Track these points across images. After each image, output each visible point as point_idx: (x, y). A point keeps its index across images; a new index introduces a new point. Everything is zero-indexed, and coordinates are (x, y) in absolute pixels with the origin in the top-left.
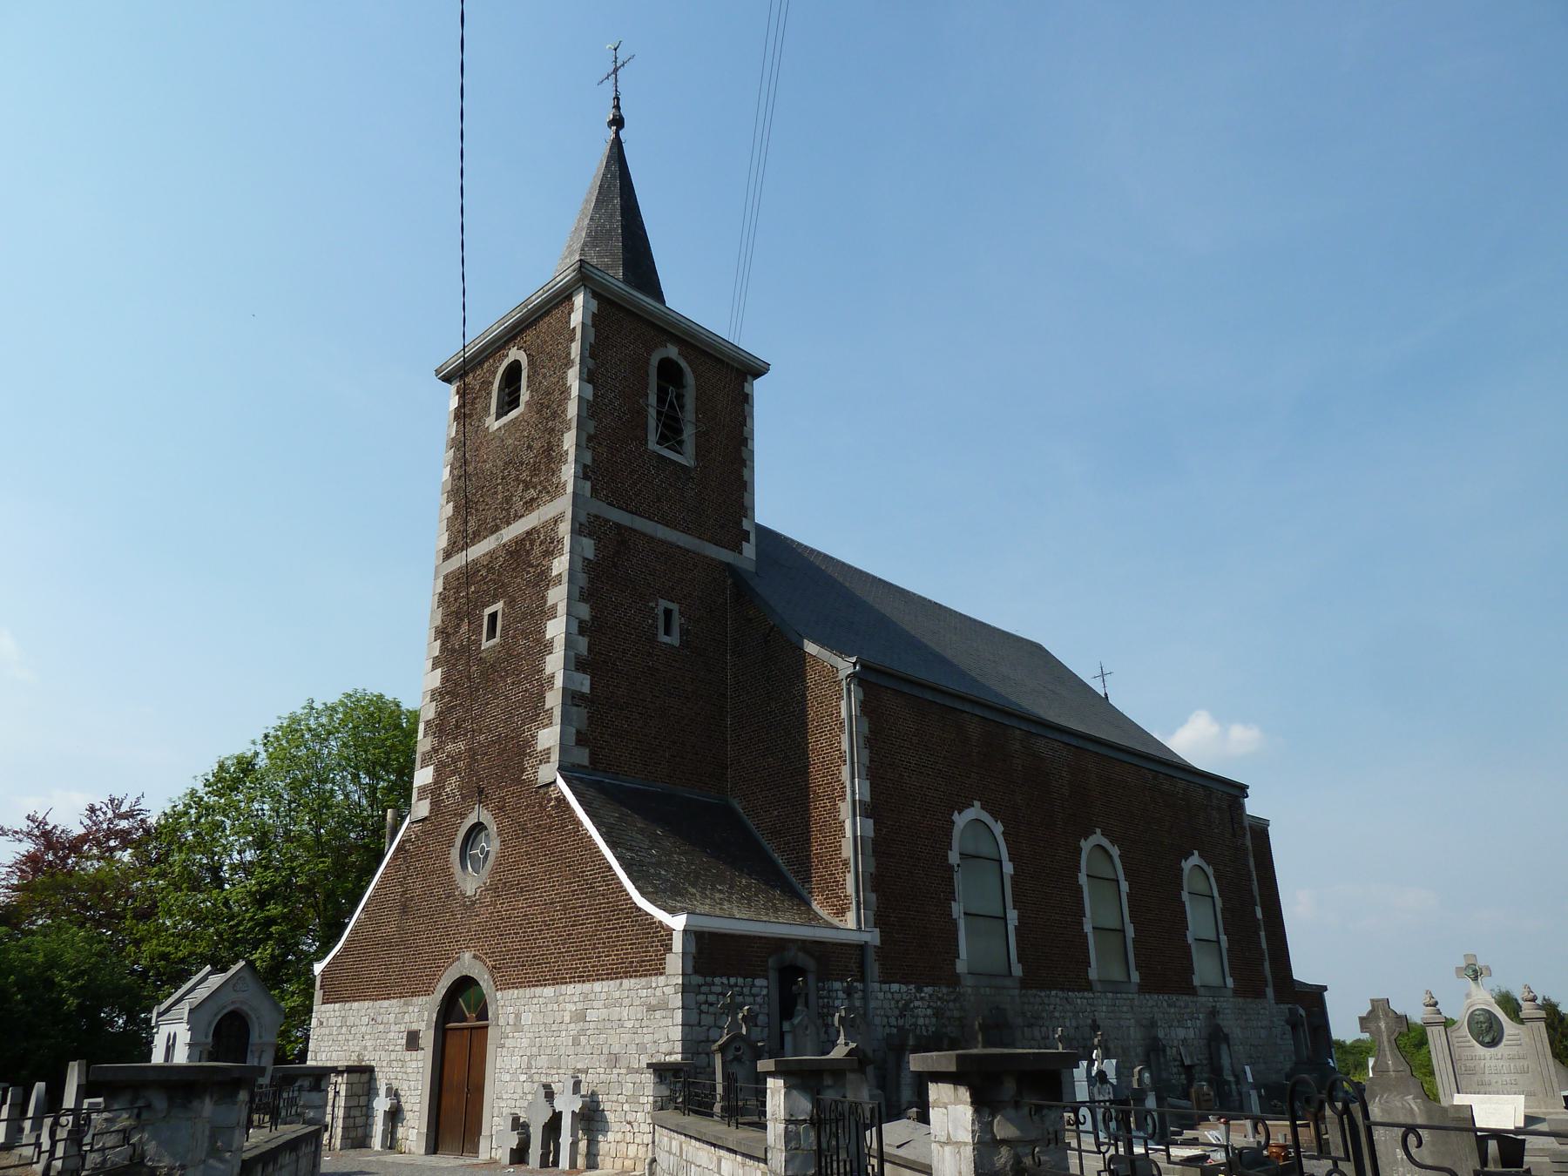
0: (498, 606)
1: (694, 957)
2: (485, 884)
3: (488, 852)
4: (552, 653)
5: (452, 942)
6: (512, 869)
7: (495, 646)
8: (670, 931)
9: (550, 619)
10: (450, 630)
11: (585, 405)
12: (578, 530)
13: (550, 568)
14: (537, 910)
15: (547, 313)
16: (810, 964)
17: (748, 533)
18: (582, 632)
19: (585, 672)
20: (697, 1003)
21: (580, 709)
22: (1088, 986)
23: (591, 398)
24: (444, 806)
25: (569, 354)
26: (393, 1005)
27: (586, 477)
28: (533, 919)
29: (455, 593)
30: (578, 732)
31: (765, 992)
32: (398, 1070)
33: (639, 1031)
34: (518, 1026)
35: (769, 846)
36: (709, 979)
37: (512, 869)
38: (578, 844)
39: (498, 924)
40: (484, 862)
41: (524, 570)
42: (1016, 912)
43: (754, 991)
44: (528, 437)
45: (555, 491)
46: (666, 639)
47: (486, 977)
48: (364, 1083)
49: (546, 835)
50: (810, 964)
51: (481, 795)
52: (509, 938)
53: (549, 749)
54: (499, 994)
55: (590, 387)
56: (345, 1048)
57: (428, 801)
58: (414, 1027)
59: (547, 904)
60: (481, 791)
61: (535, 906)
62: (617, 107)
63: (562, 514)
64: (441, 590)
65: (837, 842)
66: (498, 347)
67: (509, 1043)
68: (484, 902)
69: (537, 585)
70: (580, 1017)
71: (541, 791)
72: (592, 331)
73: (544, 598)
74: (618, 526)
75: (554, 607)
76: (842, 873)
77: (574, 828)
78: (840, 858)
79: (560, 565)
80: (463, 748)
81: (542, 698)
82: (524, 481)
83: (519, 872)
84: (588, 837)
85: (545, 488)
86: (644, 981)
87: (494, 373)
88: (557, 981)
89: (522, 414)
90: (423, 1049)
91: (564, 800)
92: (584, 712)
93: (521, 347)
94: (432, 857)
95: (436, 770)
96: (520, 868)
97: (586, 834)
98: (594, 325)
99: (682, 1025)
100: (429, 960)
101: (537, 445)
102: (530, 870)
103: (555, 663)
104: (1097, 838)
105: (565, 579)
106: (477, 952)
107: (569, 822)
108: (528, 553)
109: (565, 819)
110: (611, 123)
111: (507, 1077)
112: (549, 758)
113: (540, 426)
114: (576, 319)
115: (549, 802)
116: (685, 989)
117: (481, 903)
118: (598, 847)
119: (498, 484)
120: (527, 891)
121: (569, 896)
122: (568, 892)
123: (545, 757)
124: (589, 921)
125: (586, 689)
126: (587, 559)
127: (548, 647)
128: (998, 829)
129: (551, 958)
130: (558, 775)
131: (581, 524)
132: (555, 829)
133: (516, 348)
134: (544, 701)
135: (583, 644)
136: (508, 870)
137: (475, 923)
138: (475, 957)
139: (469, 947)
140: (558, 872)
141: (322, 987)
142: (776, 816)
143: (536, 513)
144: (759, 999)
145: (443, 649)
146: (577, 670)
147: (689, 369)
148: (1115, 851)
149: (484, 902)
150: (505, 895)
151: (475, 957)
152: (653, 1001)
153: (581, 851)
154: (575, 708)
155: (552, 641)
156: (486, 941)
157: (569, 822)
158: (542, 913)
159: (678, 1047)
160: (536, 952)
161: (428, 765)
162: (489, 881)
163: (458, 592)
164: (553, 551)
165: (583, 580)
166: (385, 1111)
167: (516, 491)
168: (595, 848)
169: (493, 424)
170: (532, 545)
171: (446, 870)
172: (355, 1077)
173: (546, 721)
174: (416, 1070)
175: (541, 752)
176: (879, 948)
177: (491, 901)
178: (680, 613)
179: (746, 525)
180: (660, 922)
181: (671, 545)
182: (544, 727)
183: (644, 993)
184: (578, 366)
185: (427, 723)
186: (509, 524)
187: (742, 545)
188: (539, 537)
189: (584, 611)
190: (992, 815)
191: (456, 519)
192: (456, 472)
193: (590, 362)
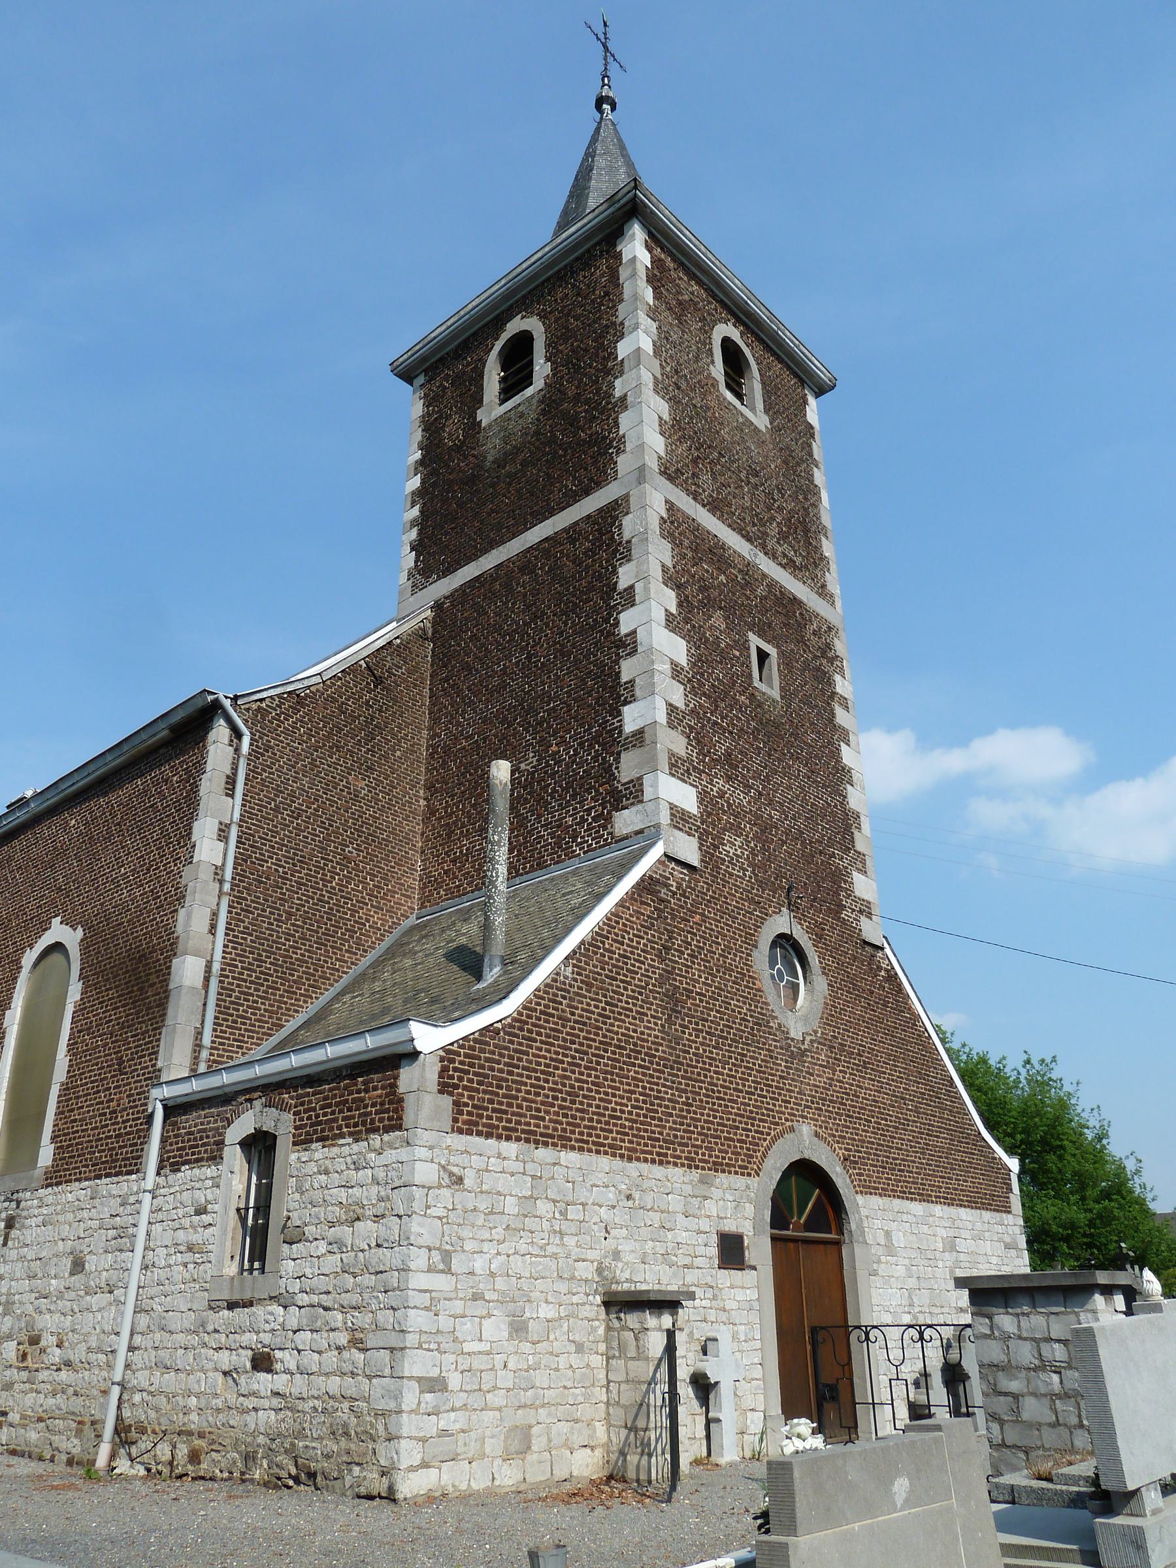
32: (705, 1303)
34: (890, 1250)
54: (859, 1198)
56: (550, 1249)
58: (730, 1227)
67: (882, 1269)
88: (924, 1198)
90: (754, 1268)
138: (817, 1135)
174: (747, 1306)
180: (1000, 1159)
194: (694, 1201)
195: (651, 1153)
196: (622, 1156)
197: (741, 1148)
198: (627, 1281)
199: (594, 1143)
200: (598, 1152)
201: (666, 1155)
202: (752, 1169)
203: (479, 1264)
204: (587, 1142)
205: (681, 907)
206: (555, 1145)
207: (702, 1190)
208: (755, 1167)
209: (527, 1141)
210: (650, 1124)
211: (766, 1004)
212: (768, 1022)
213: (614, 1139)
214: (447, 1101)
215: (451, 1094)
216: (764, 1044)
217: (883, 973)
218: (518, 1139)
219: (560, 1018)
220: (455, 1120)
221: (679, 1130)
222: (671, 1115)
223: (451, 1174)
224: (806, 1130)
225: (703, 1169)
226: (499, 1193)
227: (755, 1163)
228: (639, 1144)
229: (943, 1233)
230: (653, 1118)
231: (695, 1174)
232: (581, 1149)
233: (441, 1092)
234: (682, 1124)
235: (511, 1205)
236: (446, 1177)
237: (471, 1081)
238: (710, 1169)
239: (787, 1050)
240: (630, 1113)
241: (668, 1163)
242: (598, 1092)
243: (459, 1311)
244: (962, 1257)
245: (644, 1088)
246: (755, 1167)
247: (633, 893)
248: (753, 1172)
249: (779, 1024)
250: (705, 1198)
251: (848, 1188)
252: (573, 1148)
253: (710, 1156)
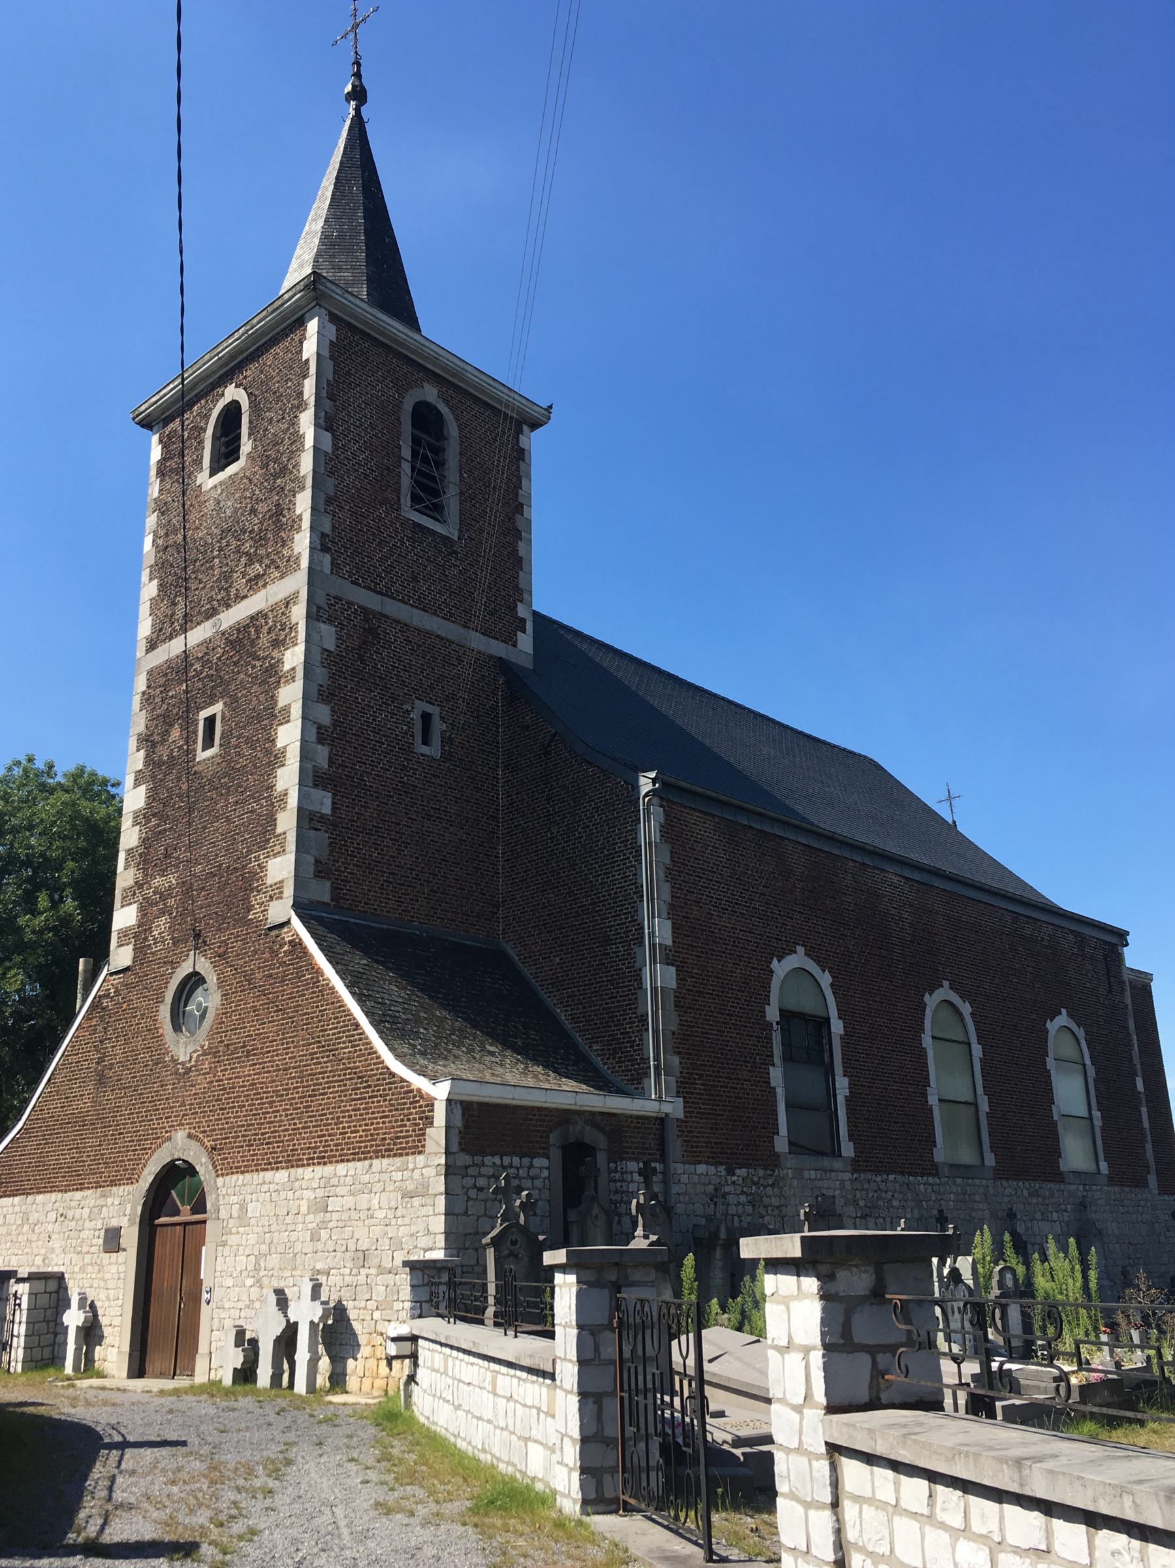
0: (217, 708)
1: (460, 1132)
2: (202, 1047)
3: (206, 1008)
4: (284, 765)
5: (162, 1118)
6: (237, 1029)
7: (213, 757)
8: (430, 1103)
9: (282, 724)
10: (156, 738)
11: (323, 457)
12: (314, 615)
13: (280, 661)
14: (267, 1078)
16: (601, 1141)
17: (524, 621)
18: (320, 741)
19: (325, 789)
20: (463, 1187)
21: (318, 833)
22: (933, 1169)
23: (329, 450)
24: (151, 953)
25: (301, 393)
26: (89, 1197)
27: (325, 549)
28: (262, 1088)
29: (161, 692)
30: (317, 862)
31: (545, 1173)
33: (393, 1222)
35: (549, 1000)
36: (478, 1159)
37: (237, 1029)
38: (318, 997)
39: (218, 1095)
40: (203, 1016)
41: (248, 663)
42: (846, 1080)
43: (533, 1172)
44: (251, 498)
45: (287, 566)
46: (424, 750)
47: (204, 1160)
48: (50, 1293)
49: (278, 987)
50: (601, 1141)
51: (198, 939)
52: (232, 1113)
53: (281, 882)
54: (220, 1181)
55: (328, 436)
56: (26, 1250)
57: (131, 947)
58: (114, 1223)
59: (280, 1070)
60: (197, 936)
61: (265, 1073)
62: (358, 75)
63: (296, 594)
64: (144, 688)
65: (632, 994)
66: (211, 384)
68: (202, 1069)
69: (264, 682)
71: (273, 933)
72: (329, 365)
73: (273, 699)
74: (365, 610)
75: (287, 709)
76: (638, 1031)
77: (312, 978)
78: (635, 1013)
79: (294, 657)
80: (174, 882)
81: (273, 821)
82: (247, 554)
83: (244, 1032)
84: (330, 989)
85: (273, 561)
86: (398, 1161)
87: (207, 417)
88: (293, 1163)
89: (242, 469)
90: (124, 1250)
91: (301, 944)
92: (324, 836)
93: (241, 384)
94: (136, 1016)
95: (141, 909)
96: (246, 1027)
97: (328, 984)
98: (331, 357)
99: (446, 1214)
100: (133, 1141)
101: (262, 508)
102: (259, 1030)
103: (288, 778)
104: (945, 992)
105: (300, 674)
107: (307, 970)
108: (253, 643)
109: (301, 967)
110: (349, 97)
111: (229, 1282)
112: (282, 893)
113: (266, 484)
114: (309, 348)
115: (281, 946)
116: (450, 1171)
117: (197, 1070)
118: (343, 1001)
119: (214, 558)
120: (254, 1055)
121: (307, 1060)
122: (305, 1055)
123: (276, 892)
124: (331, 1090)
125: (327, 809)
126: (327, 650)
127: (276, 759)
128: (825, 979)
129: (285, 1136)
130: (293, 913)
131: (319, 608)
132: (289, 980)
133: (234, 385)
134: (275, 825)
135: (322, 754)
136: (231, 1030)
137: (190, 1095)
138: (190, 1136)
139: (183, 1125)
140: (293, 1032)
142: (558, 964)
143: (263, 593)
144: (538, 1183)
145: (148, 761)
146: (316, 786)
147: (451, 417)
148: (966, 1009)
149: (202, 1069)
150: (227, 1060)
151: (190, 1136)
152: (410, 1187)
153: (322, 1006)
154: (313, 833)
155: (284, 751)
156: (204, 1117)
157: (307, 970)
158: (274, 1081)
159: (441, 1241)
160: (266, 1128)
161: (130, 904)
162: (207, 1043)
163: (166, 691)
164: (285, 639)
165: (321, 676)
166: (78, 1327)
167: (237, 566)
168: (339, 1001)
169: (206, 481)
170: (258, 632)
171: (154, 1030)
172: (40, 1286)
173: (277, 848)
174: (116, 1276)
175: (271, 886)
176: (682, 1121)
177: (211, 1068)
178: (442, 718)
179: (522, 611)
180: (419, 1090)
181: (429, 634)
182: (275, 855)
183: (398, 1176)
184: (313, 409)
185: (129, 852)
186: (228, 606)
187: (516, 635)
188: (266, 623)
189: (324, 714)
190: (818, 962)
191: (162, 600)
192: (160, 542)
193: (328, 404)
194: (96, 1210)
207: (101, 1202)
217: (286, 948)
224: (180, 1135)
229: (310, 1194)
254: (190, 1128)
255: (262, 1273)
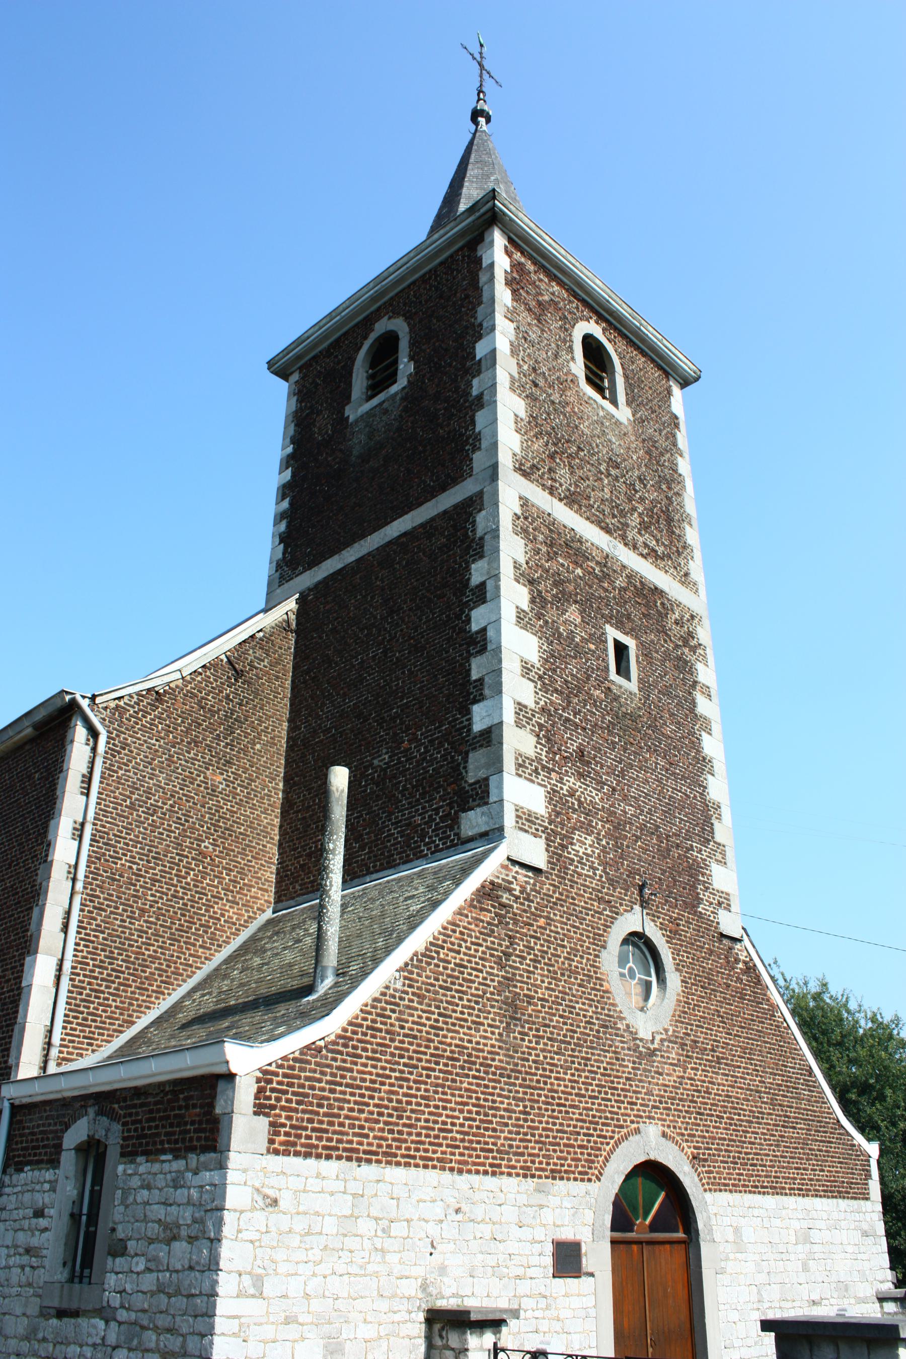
2: (666, 1030)
15: (643, 353)
34: (739, 1245)
54: (708, 1195)
56: (370, 1268)
58: (567, 1235)
67: (730, 1266)
70: (805, 1238)
90: (592, 1275)
106: (666, 1129)
129: (766, 1160)
138: (664, 1135)
139: (653, 1118)
141: (260, 1109)
160: (747, 1148)
174: (582, 1313)
180: (859, 1145)
195: (484, 1165)
196: (452, 1169)
197: (582, 1153)
198: (454, 1296)
199: (422, 1158)
200: (426, 1167)
201: (499, 1166)
202: (593, 1174)
203: (295, 1287)
204: (414, 1157)
205: (525, 911)
206: (379, 1162)
207: (539, 1198)
208: (596, 1172)
209: (349, 1159)
210: (483, 1136)
211: (614, 1005)
212: (615, 1023)
213: (443, 1153)
214: (263, 1122)
215: (267, 1115)
216: (610, 1046)
217: (741, 965)
218: (339, 1158)
219: (388, 1032)
220: (271, 1141)
221: (515, 1140)
222: (506, 1125)
223: (266, 1197)
224: (652, 1130)
225: (540, 1177)
226: (317, 1214)
227: (596, 1168)
228: (470, 1156)
229: (796, 1225)
230: (486, 1129)
231: (531, 1183)
232: (407, 1165)
233: (256, 1113)
234: (518, 1133)
235: (330, 1226)
236: (259, 1199)
237: (288, 1101)
238: (547, 1177)
239: (635, 1051)
240: (462, 1125)
241: (502, 1173)
242: (427, 1106)
243: (271, 1336)
244: (816, 1248)
245: (478, 1099)
246: (596, 1172)
247: (472, 900)
248: (594, 1178)
249: (628, 1026)
250: (541, 1207)
251: (696, 1186)
252: (398, 1164)
253: (548, 1164)
254: (663, 1125)
255: (766, 1305)
